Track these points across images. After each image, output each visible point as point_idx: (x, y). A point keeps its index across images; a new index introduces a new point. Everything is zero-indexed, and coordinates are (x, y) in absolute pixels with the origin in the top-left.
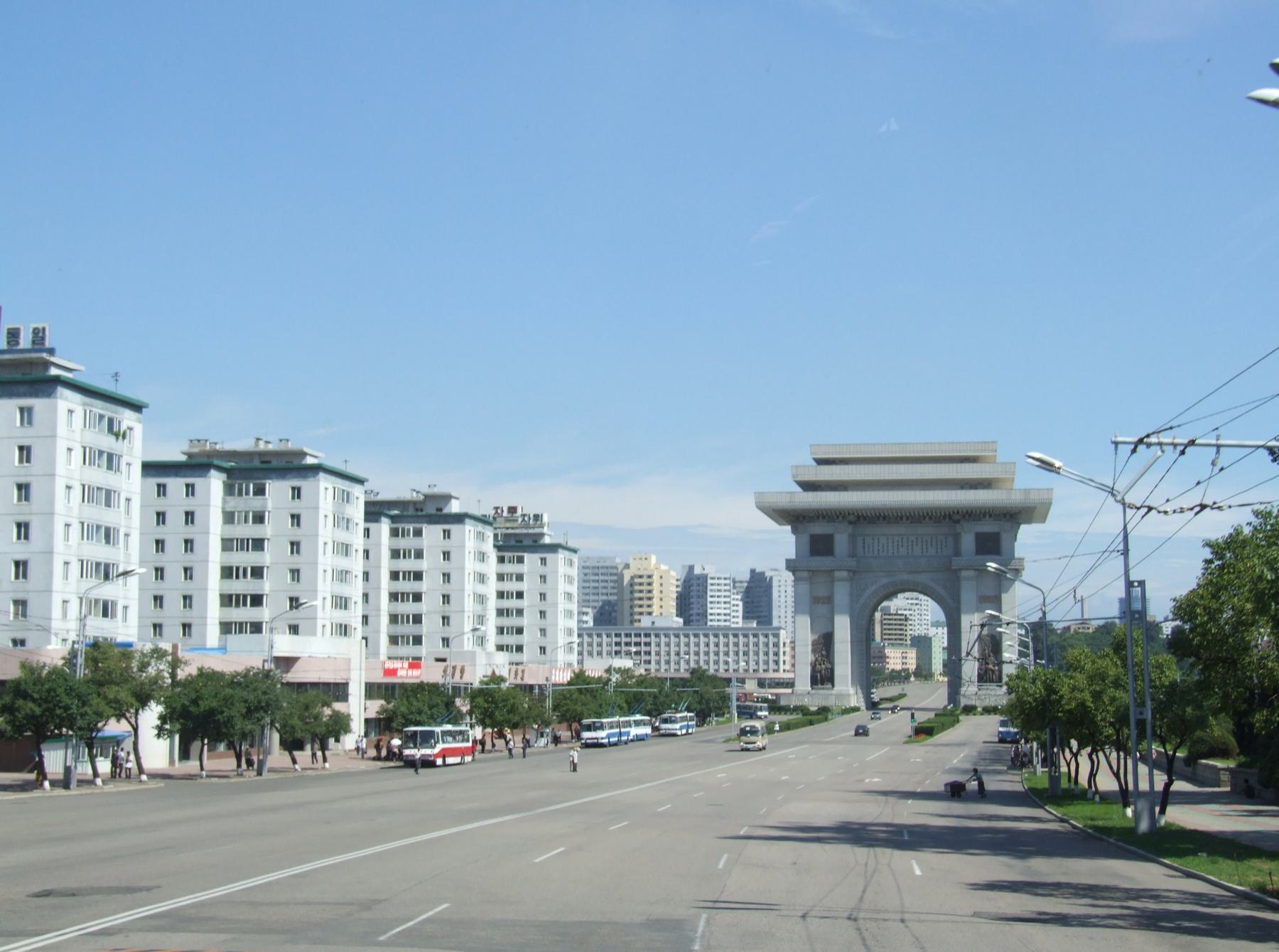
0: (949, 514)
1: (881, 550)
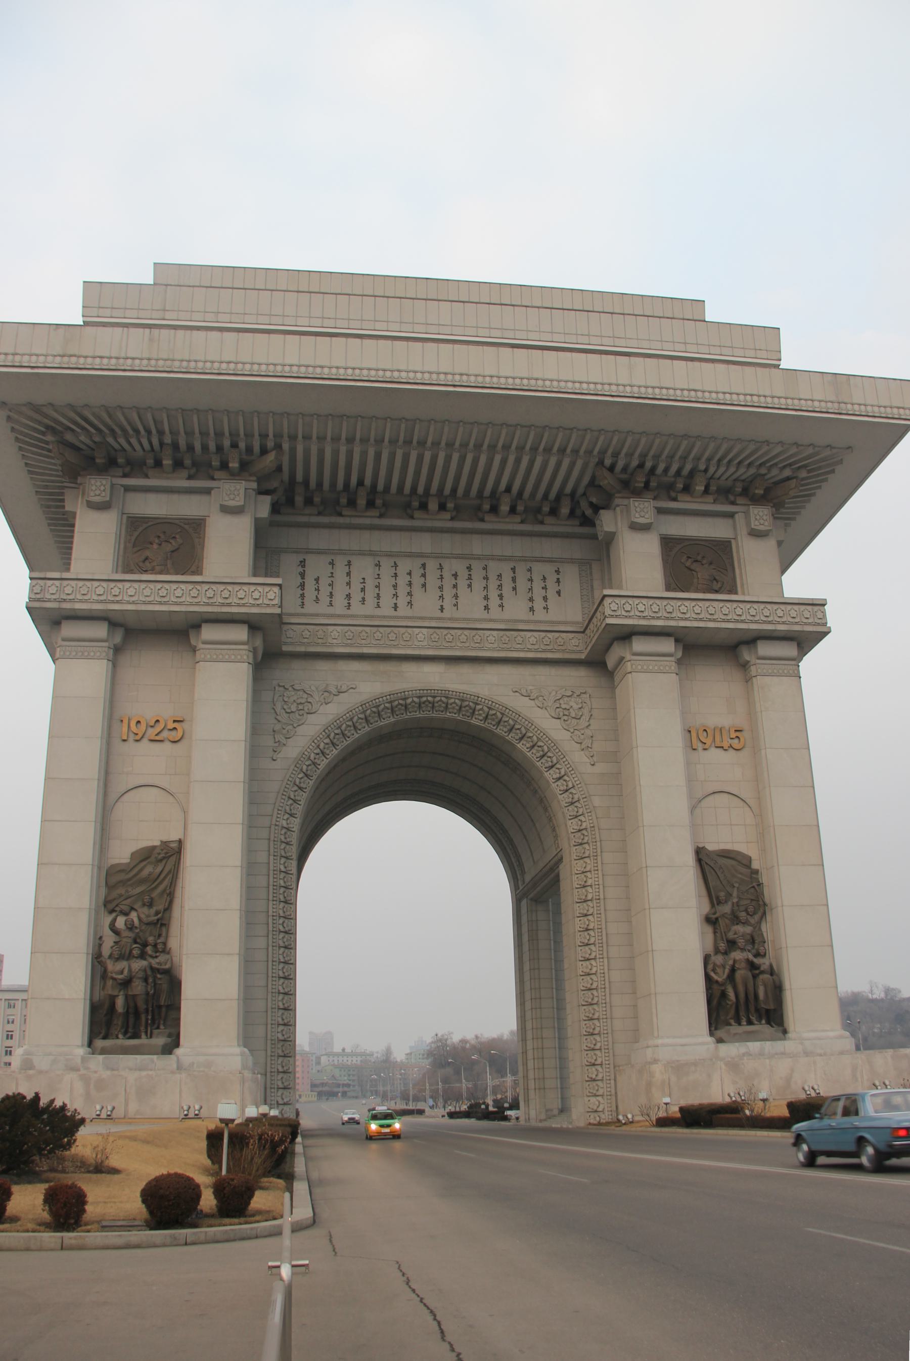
0: (573, 494)
1: (356, 597)
